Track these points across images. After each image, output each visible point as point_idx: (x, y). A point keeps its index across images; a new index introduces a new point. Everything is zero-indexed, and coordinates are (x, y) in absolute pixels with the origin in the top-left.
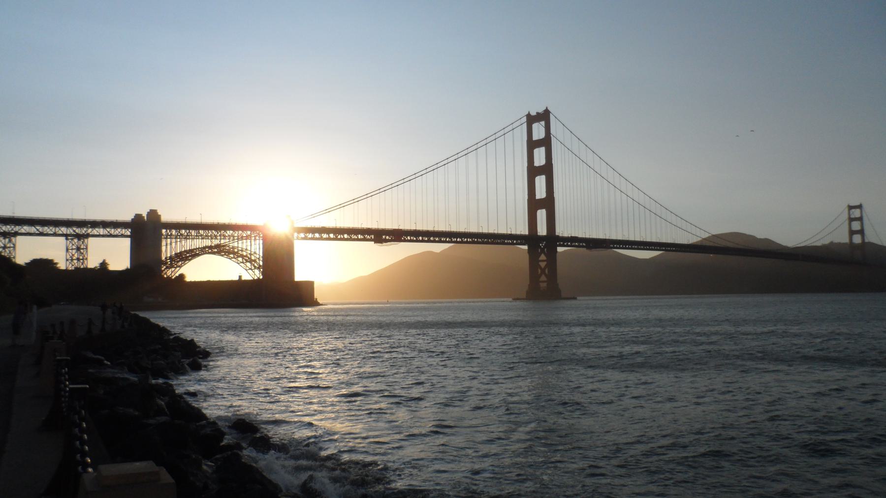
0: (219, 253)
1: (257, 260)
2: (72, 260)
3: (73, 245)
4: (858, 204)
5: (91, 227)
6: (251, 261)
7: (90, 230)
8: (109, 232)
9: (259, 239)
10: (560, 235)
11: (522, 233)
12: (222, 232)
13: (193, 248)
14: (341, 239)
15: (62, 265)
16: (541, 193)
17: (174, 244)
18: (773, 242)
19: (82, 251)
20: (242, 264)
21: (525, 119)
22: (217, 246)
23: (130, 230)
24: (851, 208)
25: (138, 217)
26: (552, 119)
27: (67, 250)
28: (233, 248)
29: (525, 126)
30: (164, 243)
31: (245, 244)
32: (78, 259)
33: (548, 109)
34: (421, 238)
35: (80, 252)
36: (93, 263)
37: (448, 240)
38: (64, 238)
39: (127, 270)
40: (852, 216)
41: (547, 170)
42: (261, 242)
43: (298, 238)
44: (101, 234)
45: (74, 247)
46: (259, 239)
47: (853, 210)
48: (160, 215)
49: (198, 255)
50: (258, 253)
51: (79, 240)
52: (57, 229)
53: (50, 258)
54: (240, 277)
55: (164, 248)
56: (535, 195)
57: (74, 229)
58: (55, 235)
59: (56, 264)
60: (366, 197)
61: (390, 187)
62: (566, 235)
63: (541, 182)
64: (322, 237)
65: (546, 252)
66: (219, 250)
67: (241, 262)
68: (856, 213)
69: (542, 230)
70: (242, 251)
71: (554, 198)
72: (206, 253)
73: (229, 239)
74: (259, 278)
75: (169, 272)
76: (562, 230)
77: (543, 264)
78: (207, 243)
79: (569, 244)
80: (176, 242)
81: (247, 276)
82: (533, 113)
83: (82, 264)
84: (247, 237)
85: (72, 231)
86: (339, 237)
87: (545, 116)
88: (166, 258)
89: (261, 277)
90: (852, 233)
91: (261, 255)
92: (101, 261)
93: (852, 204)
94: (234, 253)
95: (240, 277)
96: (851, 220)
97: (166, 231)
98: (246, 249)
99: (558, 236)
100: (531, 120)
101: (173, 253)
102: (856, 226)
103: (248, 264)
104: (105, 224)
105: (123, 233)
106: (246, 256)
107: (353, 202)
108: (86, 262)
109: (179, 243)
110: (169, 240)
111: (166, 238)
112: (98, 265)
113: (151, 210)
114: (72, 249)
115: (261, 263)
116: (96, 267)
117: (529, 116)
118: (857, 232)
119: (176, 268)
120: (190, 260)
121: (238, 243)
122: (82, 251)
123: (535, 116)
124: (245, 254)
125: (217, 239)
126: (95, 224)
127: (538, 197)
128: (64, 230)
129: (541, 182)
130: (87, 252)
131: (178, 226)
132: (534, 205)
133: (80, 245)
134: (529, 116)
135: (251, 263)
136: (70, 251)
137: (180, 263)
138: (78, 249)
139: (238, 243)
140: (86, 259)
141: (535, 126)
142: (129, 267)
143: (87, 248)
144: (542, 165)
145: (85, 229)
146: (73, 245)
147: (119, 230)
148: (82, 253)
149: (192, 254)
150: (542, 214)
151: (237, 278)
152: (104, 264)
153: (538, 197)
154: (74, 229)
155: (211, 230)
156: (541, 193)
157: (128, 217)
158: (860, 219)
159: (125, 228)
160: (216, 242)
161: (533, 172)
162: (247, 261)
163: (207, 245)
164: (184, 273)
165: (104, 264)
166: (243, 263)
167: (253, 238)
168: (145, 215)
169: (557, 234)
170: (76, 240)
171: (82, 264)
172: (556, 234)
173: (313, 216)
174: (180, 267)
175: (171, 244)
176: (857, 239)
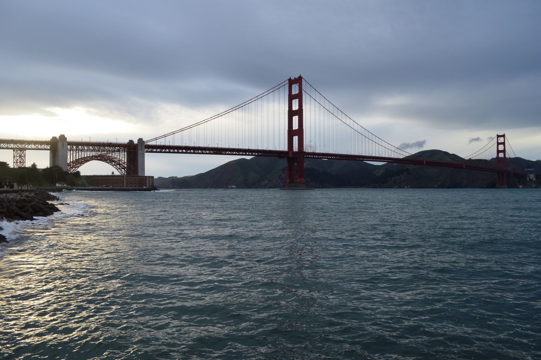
0: (101, 160)
1: (123, 164)
2: (17, 162)
3: (17, 154)
4: (502, 134)
5: (27, 144)
6: (119, 164)
7: (27, 146)
8: (18, 146)
9: (124, 152)
10: (307, 151)
11: (284, 150)
12: (113, 147)
13: (86, 156)
14: (189, 153)
15: (11, 165)
16: (295, 126)
17: (74, 155)
19: (22, 157)
20: (114, 166)
21: (287, 82)
22: (100, 156)
23: (49, 146)
24: (498, 136)
25: (54, 138)
26: (303, 81)
27: (14, 157)
28: (109, 157)
29: (288, 85)
30: (69, 153)
31: (116, 154)
32: (20, 162)
33: (302, 76)
34: (247, 153)
35: (21, 158)
36: (28, 164)
37: (188, 152)
38: (12, 150)
39: (47, 169)
40: (499, 141)
41: (300, 113)
42: (126, 153)
43: (147, 152)
44: (33, 148)
45: (18, 155)
46: (124, 152)
48: (66, 138)
49: (88, 161)
50: (123, 159)
51: (21, 151)
52: (8, 145)
53: (5, 162)
54: (113, 173)
55: (69, 156)
56: (292, 128)
57: (18, 145)
58: (7, 148)
59: (8, 165)
60: (188, 128)
61: (203, 122)
62: (309, 151)
63: (296, 119)
64: (179, 151)
66: (101, 158)
67: (114, 165)
68: (501, 140)
69: (296, 148)
70: (114, 158)
72: (93, 160)
73: (107, 152)
74: (124, 174)
75: (72, 171)
76: (308, 148)
78: (94, 153)
80: (76, 153)
81: (117, 173)
82: (293, 78)
83: (22, 165)
84: (118, 151)
85: (16, 146)
86: (188, 152)
87: (299, 80)
88: (70, 162)
89: (126, 174)
90: (499, 152)
91: (126, 161)
92: (32, 164)
93: (499, 134)
94: (110, 160)
95: (113, 173)
96: (498, 144)
97: (70, 147)
98: (117, 158)
99: (305, 152)
100: (291, 82)
101: (74, 159)
102: (501, 147)
103: (118, 166)
104: (35, 143)
105: (46, 147)
106: (117, 161)
107: (180, 130)
108: (24, 164)
109: (77, 154)
110: (72, 152)
111: (70, 151)
112: (31, 166)
113: (61, 135)
114: (17, 156)
115: (126, 166)
116: (30, 167)
117: (290, 80)
118: (501, 151)
119: (76, 168)
120: (84, 163)
121: (112, 154)
122: (22, 157)
123: (293, 80)
124: (116, 160)
125: (100, 151)
126: (29, 143)
127: (294, 129)
128: (12, 145)
129: (296, 119)
130: (25, 158)
131: (77, 144)
132: (291, 133)
133: (21, 154)
134: (290, 80)
135: (119, 165)
136: (16, 157)
137: (78, 165)
138: (20, 156)
139: (112, 154)
140: (25, 162)
141: (293, 86)
142: (49, 167)
143: (25, 156)
144: (296, 109)
145: (24, 145)
146: (17, 154)
147: (43, 146)
148: (23, 159)
149: (86, 160)
150: (296, 139)
151: (110, 174)
152: (34, 166)
153: (294, 129)
154: (18, 145)
155: (11, 143)
156: (295, 126)
157: (48, 138)
158: (504, 144)
159: (47, 145)
160: (99, 153)
161: (291, 114)
162: (117, 165)
163: (94, 155)
164: (79, 171)
165: (34, 166)
166: (115, 165)
167: (121, 151)
168: (58, 137)
169: (304, 151)
170: (19, 152)
171: (22, 165)
173: (156, 139)
174: (78, 167)
175: (73, 153)
176: (501, 155)
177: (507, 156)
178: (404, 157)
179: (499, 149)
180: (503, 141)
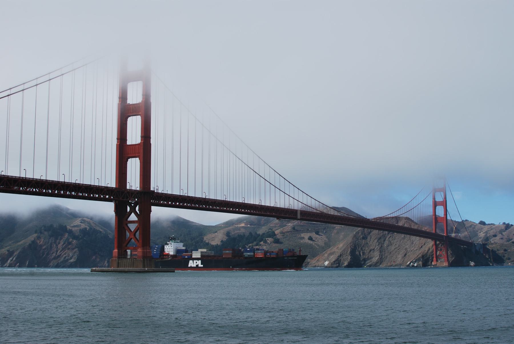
18: (351, 211)
56: (126, 140)
62: (160, 191)
65: (138, 212)
77: (133, 227)
79: (107, 197)
90: (435, 204)
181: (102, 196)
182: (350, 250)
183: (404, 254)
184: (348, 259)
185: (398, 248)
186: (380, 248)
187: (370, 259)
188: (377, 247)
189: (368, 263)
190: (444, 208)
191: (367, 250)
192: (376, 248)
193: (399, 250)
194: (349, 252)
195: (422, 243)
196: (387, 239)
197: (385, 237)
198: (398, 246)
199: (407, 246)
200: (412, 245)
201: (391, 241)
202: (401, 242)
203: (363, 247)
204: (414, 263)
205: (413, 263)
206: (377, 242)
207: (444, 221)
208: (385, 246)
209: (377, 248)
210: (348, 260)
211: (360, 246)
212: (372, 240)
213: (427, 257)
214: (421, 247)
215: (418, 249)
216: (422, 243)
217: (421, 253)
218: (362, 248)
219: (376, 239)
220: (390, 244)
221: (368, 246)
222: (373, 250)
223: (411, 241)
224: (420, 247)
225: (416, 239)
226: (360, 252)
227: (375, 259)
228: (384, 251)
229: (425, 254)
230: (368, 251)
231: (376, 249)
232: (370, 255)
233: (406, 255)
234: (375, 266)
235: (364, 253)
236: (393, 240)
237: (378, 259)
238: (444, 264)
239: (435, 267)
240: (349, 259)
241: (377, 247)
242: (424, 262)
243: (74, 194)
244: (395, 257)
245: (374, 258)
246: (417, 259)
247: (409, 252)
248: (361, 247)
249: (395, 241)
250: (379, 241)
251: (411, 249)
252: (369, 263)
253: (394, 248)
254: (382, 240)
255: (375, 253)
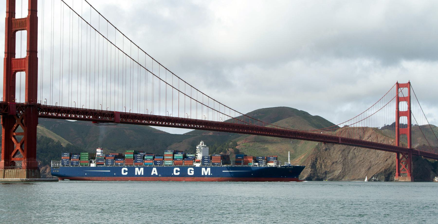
4: (407, 82)
10: (43, 103)
24: (399, 85)
40: (400, 95)
47: (402, 88)
68: (404, 92)
71: (37, 58)
90: (399, 114)
96: (399, 100)
118: (404, 114)
127: (17, 56)
169: (38, 103)
172: (38, 103)
176: (404, 120)
177: (413, 123)
178: (229, 118)
179: (400, 110)
180: (406, 95)
181: (87, 117)
182: (310, 162)
183: (368, 167)
184: (308, 172)
185: (363, 161)
186: (344, 161)
187: (333, 172)
188: (340, 159)
189: (330, 176)
190: (408, 119)
191: (329, 163)
192: (339, 161)
193: (364, 163)
194: (309, 164)
195: (387, 156)
196: (351, 151)
197: (350, 149)
198: (363, 158)
199: (372, 159)
200: (377, 158)
201: (356, 153)
202: (366, 154)
203: (325, 160)
204: (376, 177)
205: (375, 177)
206: (340, 154)
207: (407, 132)
208: (350, 158)
209: (340, 161)
210: (308, 173)
211: (322, 158)
212: (335, 151)
213: (391, 171)
214: (386, 160)
215: (383, 162)
216: (387, 156)
217: (384, 167)
218: (324, 160)
219: (339, 150)
220: (354, 157)
221: (331, 158)
222: (336, 163)
223: (377, 153)
224: (385, 160)
225: (382, 153)
226: (322, 164)
227: (337, 173)
228: (347, 164)
229: (388, 168)
230: (331, 164)
231: (339, 162)
232: (333, 168)
233: (370, 168)
234: (337, 179)
235: (325, 166)
236: (358, 152)
237: (340, 172)
238: (407, 179)
239: (397, 181)
240: (310, 172)
241: (340, 159)
242: (387, 176)
243: (54, 115)
244: (358, 171)
245: (336, 171)
246: (379, 173)
247: (373, 166)
248: (323, 159)
249: (360, 153)
250: (343, 153)
251: (375, 163)
252: (331, 176)
253: (358, 161)
254: (346, 152)
255: (338, 166)
